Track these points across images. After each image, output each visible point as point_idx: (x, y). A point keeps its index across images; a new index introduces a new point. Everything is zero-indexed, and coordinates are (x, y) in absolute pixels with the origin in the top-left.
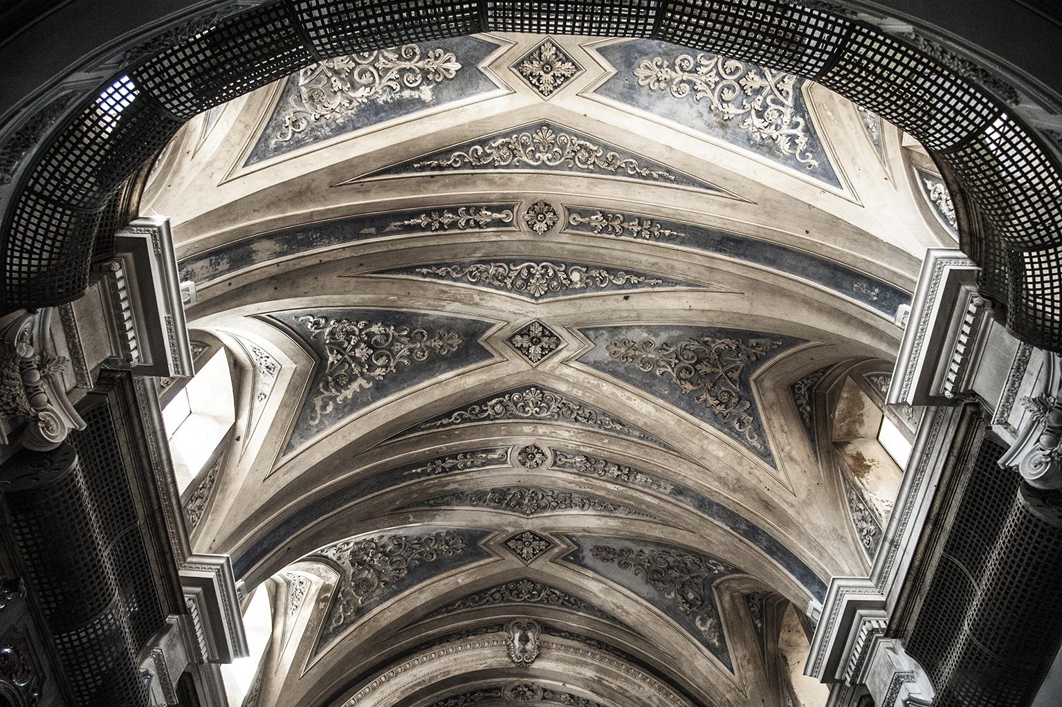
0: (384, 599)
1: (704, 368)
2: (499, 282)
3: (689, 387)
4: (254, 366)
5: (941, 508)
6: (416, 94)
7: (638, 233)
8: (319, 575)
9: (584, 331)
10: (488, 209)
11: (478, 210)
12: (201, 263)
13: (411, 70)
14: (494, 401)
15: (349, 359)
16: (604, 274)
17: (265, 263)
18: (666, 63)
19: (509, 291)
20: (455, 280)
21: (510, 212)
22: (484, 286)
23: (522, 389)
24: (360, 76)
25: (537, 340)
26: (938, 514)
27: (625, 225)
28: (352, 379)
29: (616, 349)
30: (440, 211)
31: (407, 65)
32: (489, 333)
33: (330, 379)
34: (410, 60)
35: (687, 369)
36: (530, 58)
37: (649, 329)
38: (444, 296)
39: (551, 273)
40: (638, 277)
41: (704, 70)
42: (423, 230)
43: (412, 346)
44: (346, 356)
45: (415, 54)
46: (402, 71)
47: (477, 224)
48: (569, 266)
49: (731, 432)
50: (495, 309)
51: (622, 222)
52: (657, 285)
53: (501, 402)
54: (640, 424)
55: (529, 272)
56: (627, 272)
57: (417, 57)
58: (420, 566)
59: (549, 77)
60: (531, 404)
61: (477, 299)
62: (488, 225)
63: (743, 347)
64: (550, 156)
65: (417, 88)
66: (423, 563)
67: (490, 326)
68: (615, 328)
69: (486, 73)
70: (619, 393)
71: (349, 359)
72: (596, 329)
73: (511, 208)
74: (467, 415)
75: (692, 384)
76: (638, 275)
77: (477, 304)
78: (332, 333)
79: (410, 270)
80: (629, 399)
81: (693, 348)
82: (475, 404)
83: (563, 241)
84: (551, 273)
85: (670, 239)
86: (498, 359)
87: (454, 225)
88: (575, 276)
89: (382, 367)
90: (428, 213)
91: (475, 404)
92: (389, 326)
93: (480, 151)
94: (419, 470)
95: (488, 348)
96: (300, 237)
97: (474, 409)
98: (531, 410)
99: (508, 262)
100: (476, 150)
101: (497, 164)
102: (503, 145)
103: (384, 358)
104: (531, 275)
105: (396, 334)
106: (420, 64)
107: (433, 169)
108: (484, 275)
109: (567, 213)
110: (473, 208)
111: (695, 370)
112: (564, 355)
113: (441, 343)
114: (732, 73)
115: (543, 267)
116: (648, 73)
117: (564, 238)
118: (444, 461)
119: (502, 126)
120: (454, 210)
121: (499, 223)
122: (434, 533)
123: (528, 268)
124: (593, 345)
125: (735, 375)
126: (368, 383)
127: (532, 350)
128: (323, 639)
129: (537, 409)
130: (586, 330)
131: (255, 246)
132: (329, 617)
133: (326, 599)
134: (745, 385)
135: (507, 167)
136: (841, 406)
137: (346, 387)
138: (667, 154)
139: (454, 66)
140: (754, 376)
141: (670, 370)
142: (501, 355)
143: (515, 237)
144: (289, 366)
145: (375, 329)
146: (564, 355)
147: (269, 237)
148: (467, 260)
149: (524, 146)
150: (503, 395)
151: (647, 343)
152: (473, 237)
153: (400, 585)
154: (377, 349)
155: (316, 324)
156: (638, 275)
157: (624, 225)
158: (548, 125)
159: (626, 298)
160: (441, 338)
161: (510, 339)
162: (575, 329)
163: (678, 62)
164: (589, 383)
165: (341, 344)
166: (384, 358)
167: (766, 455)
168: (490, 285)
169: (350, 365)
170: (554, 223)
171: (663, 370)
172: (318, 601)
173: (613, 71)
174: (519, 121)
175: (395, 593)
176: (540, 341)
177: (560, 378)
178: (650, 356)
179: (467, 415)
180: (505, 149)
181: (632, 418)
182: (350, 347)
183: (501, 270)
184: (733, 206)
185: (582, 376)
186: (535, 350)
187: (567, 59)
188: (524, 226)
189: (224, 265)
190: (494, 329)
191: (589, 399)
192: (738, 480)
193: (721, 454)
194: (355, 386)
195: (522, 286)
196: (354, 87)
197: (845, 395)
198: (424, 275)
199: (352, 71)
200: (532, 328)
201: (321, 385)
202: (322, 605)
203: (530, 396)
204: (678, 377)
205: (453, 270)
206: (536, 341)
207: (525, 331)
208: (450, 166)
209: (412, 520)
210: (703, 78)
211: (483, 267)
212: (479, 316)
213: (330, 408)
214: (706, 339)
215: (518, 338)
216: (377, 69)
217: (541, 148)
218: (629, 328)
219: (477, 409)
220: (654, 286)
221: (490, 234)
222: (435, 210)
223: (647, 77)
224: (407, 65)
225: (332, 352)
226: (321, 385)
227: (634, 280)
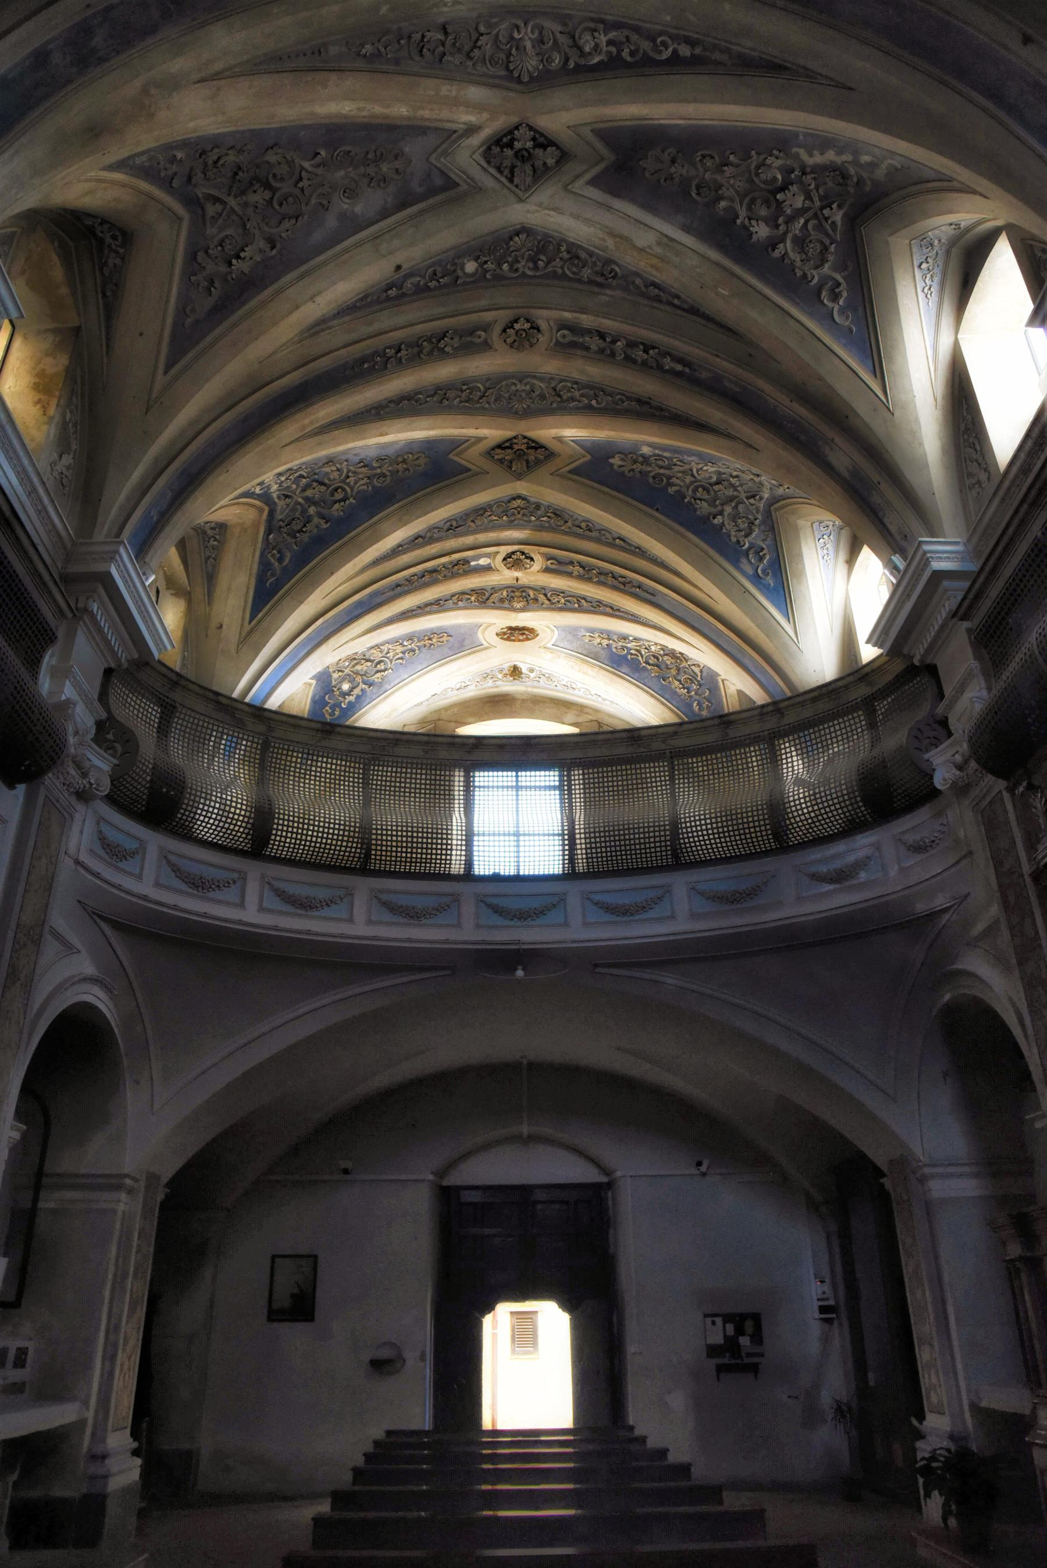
1: (258, 197)
2: (575, 253)
3: (271, 157)
4: (948, 252)
5: (17, 538)
6: (657, 451)
7: (399, 350)
9: (450, 184)
10: (587, 349)
11: (602, 351)
12: (893, 529)
13: (661, 467)
14: (596, 60)
15: (816, 199)
16: (433, 284)
17: (843, 456)
18: (400, 474)
19: (563, 240)
20: (636, 274)
21: (561, 340)
22: (598, 255)
23: (543, 80)
24: (711, 478)
25: (522, 156)
26: (13, 531)
27: (416, 350)
28: (821, 170)
29: (397, 164)
30: (644, 363)
31: (662, 471)
32: (598, 169)
33: (852, 190)
34: (659, 474)
35: (282, 179)
36: (538, 463)
37: (353, 225)
38: (655, 261)
39: (505, 266)
40: (390, 294)
41: (362, 482)
42: (669, 354)
43: (719, 178)
44: (818, 204)
45: (654, 478)
46: (668, 468)
47: (602, 336)
48: (479, 279)
49: (184, 144)
50: (588, 221)
51: (421, 352)
52: (361, 299)
53: (582, 54)
54: (334, 77)
55: (535, 263)
56: (404, 295)
57: (652, 474)
59: (516, 447)
60: (528, 44)
61: (610, 243)
62: (589, 332)
63: (223, 268)
64: (513, 387)
65: (655, 455)
67: (594, 182)
68: (403, 206)
69: (583, 452)
70: (378, 109)
71: (816, 199)
72: (432, 192)
73: (558, 343)
74: (646, 45)
75: (268, 162)
76: (388, 299)
77: (612, 234)
78: (823, 261)
79: (694, 311)
80: (359, 109)
81: (287, 224)
82: (628, 65)
83: (491, 310)
84: (505, 266)
85: (363, 360)
86: (586, 132)
87: (632, 344)
88: (471, 267)
89: (769, 166)
90: (660, 367)
91: (628, 65)
92: (744, 227)
93: (594, 402)
95: (599, 145)
96: (803, 438)
97: (632, 54)
98: (527, 36)
99: (564, 276)
100: (598, 403)
101: (575, 386)
102: (567, 400)
103: (763, 176)
104: (534, 260)
105: (737, 207)
106: (649, 469)
107: (648, 403)
108: (598, 269)
109: (489, 341)
110: (606, 355)
111: (267, 186)
112: (475, 140)
113: (673, 170)
114: (336, 490)
115: (517, 270)
116: (417, 462)
117: (489, 316)
119: (567, 419)
120: (628, 358)
121: (573, 328)
123: (536, 268)
124: (432, 159)
125: (211, 210)
126: (797, 155)
127: (529, 144)
129: (516, 35)
130: (444, 190)
131: (846, 474)
134: (192, 202)
135: (561, 381)
136: (58, 272)
137: (832, 168)
138: (385, 429)
139: (616, 461)
140: (185, 224)
141: (306, 165)
142: (579, 135)
143: (555, 314)
144: (899, 242)
145: (761, 231)
146: (475, 140)
147: (828, 468)
148: (619, 293)
149: (542, 397)
150: (579, 69)
151: (351, 192)
152: (608, 324)
154: (769, 192)
155: (835, 297)
156: (388, 299)
157: (416, 350)
158: (516, 413)
159: (398, 268)
160: (670, 178)
161: (564, 156)
162: (464, 187)
163: (389, 479)
164: (432, 109)
165: (820, 227)
166: (763, 176)
167: (119, 166)
168: (591, 254)
169: (817, 188)
170: (504, 331)
171: (318, 159)
173: (451, 456)
174: (550, 419)
176: (517, 154)
177: (479, 107)
178: (342, 173)
179: (646, 45)
180: (565, 397)
181: (350, 82)
182: (810, 213)
183: (575, 269)
184: (304, 427)
185: (445, 114)
186: (524, 142)
187: (501, 461)
188: (543, 325)
189: (875, 499)
190: (588, 176)
191: (428, 87)
192: (151, 116)
193: (191, 125)
194: (818, 159)
195: (545, 247)
196: (719, 473)
197: (64, 290)
198: (678, 297)
199: (718, 483)
200: (528, 180)
201: (868, 189)
203: (532, 63)
204: (290, 163)
205: (637, 287)
206: (524, 157)
207: (540, 174)
208: (629, 399)
210: (361, 476)
211: (600, 279)
212: (609, 208)
213: (865, 159)
214: (274, 252)
215: (551, 162)
216: (693, 475)
217: (524, 395)
218: (384, 214)
219: (625, 54)
220: (366, 297)
221: (587, 320)
222: (651, 367)
223: (417, 459)
224: (662, 471)
225: (833, 223)
226: (868, 189)
227: (393, 292)
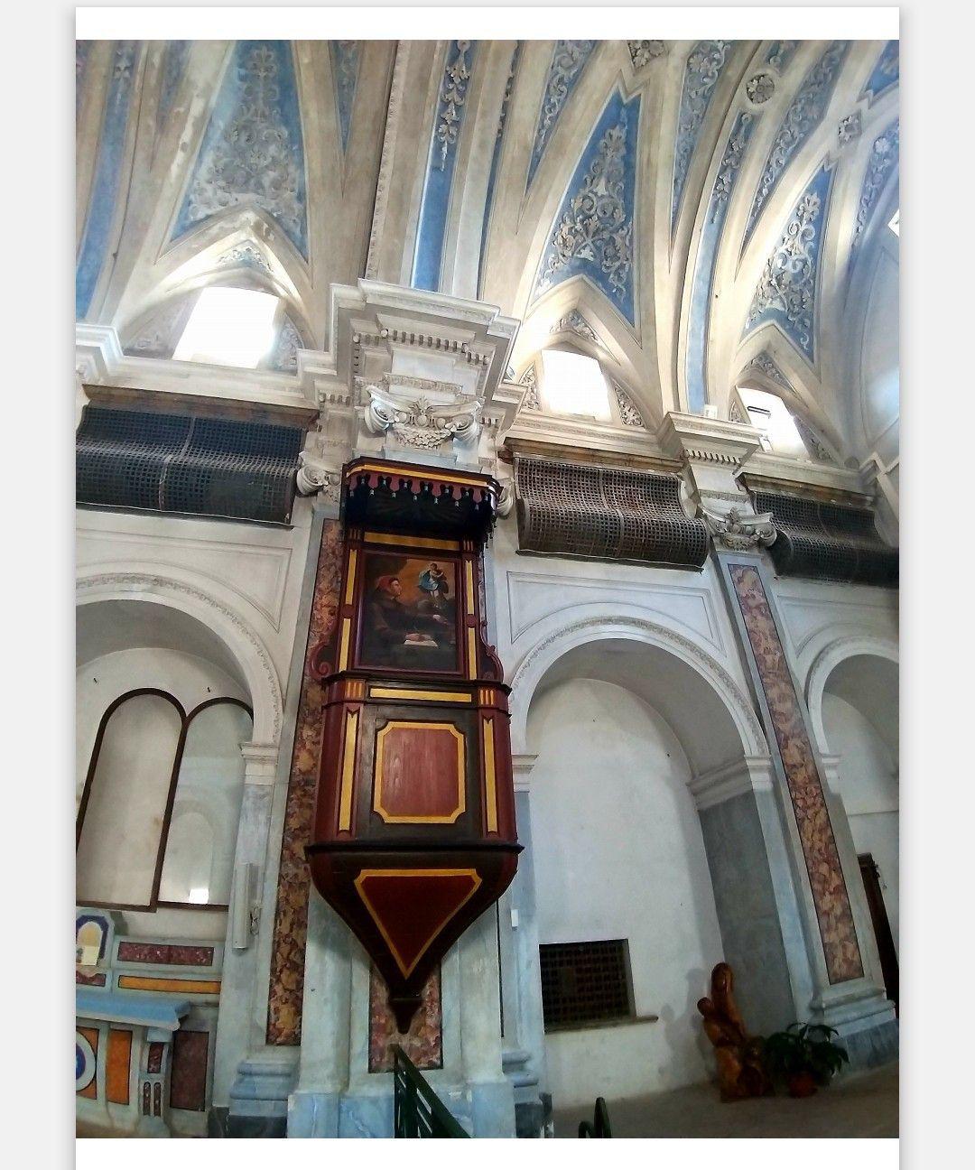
0: (301, 164)
8: (235, 230)
58: (282, 107)
66: (281, 104)
94: (119, 96)
118: (119, 69)
122: (239, 83)
128: (301, 248)
132: (288, 232)
133: (268, 232)
153: (295, 141)
172: (265, 239)
175: (301, 148)
202: (271, 237)
209: (182, 110)
